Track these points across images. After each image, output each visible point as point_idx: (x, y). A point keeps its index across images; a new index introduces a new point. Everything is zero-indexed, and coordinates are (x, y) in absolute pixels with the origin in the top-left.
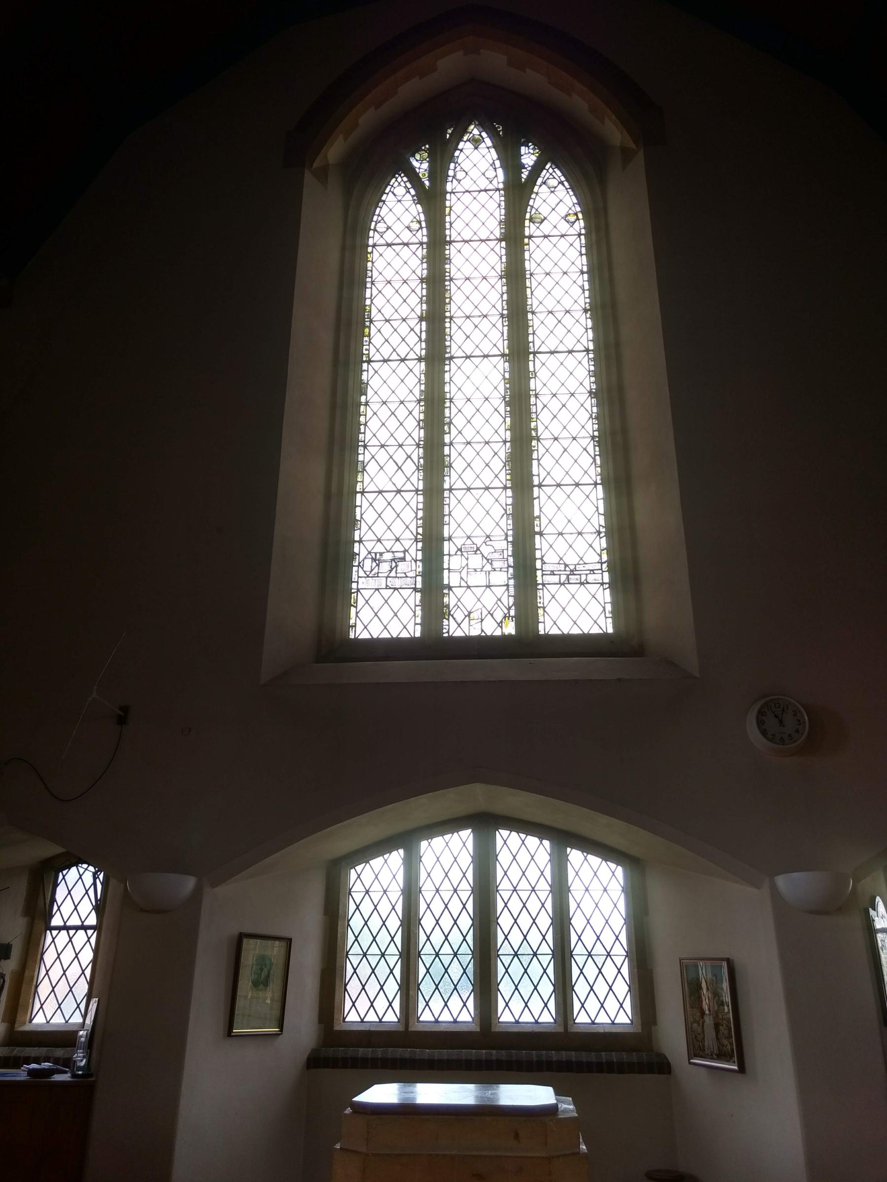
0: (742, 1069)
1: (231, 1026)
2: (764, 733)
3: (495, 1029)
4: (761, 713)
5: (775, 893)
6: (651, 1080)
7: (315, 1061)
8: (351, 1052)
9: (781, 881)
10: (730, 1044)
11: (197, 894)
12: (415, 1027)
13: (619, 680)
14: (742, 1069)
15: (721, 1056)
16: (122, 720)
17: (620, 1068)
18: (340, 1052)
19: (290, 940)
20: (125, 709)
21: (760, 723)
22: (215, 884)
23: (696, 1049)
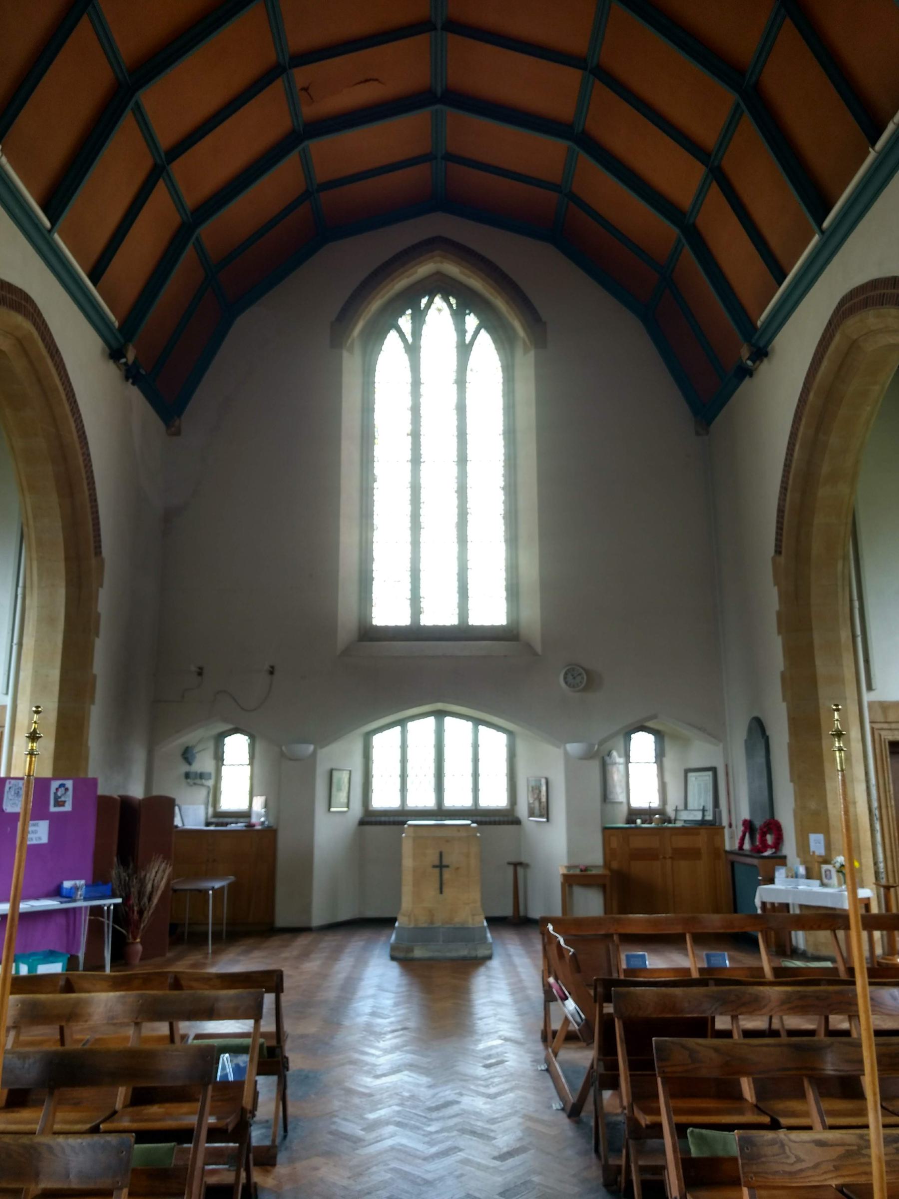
0: (548, 821)
1: (330, 806)
2: (566, 683)
3: (444, 808)
4: (566, 674)
5: (566, 753)
7: (362, 823)
8: (378, 819)
10: (544, 812)
11: (314, 753)
12: (406, 808)
13: (505, 656)
14: (548, 821)
15: (541, 816)
16: (272, 673)
17: (499, 823)
18: (373, 819)
19: (350, 771)
20: (272, 667)
21: (565, 678)
22: (322, 747)
23: (532, 814)
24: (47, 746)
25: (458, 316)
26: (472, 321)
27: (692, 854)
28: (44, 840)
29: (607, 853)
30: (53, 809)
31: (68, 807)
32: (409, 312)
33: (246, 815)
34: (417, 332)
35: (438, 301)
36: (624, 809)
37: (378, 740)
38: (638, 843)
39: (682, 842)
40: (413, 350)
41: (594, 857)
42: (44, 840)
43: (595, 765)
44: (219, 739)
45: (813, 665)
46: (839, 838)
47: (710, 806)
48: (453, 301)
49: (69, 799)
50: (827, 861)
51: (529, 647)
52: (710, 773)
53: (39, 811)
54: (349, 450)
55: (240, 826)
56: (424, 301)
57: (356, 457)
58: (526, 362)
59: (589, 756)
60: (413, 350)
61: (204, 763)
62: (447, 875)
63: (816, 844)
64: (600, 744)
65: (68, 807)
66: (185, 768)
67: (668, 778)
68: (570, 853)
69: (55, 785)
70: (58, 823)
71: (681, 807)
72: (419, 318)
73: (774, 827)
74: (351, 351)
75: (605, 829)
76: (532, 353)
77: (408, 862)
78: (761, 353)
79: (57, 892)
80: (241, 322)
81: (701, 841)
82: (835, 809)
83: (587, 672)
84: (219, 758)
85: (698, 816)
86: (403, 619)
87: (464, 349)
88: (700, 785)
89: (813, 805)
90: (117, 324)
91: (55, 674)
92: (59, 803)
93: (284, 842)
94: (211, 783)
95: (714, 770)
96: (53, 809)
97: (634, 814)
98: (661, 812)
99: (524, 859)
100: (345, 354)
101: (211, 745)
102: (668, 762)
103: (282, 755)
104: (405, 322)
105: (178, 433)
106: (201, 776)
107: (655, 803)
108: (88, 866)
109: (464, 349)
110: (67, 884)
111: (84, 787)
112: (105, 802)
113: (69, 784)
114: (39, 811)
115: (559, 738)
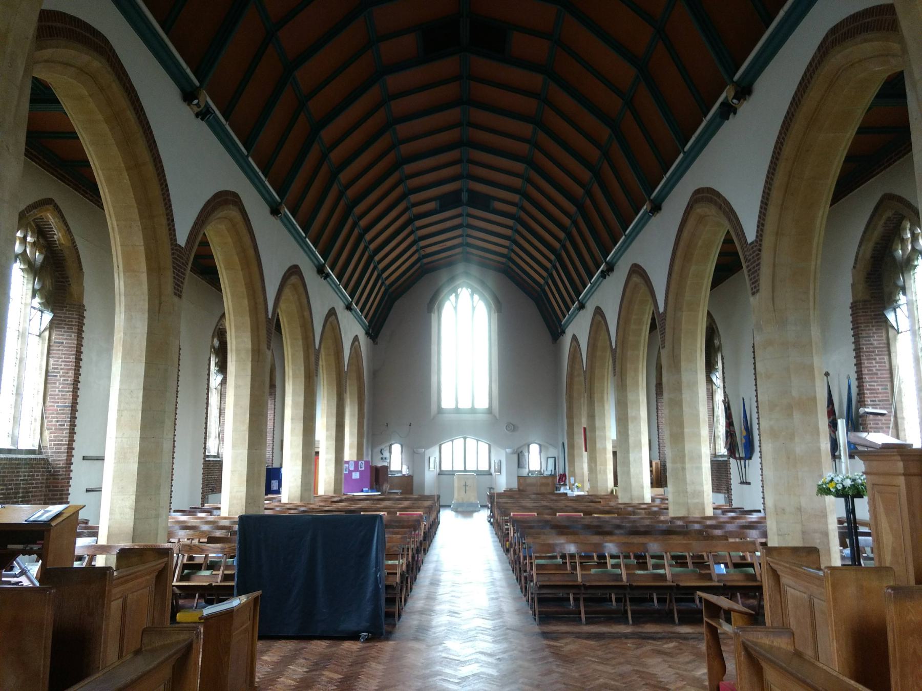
5: (506, 452)
6: (490, 476)
7: (439, 474)
9: (507, 450)
23: (495, 472)
24: (355, 451)
25: (472, 295)
26: (476, 297)
27: (547, 485)
28: (358, 477)
29: (519, 483)
30: (360, 469)
31: (363, 469)
32: (454, 294)
33: (401, 472)
34: (456, 302)
35: (464, 289)
36: (527, 470)
37: (443, 446)
38: (529, 481)
39: (544, 481)
40: (455, 308)
41: (515, 485)
42: (358, 477)
43: (515, 457)
44: (390, 446)
45: (573, 430)
46: (578, 478)
47: (553, 469)
48: (469, 290)
49: (363, 466)
50: (573, 485)
51: (495, 416)
52: (549, 459)
53: (356, 469)
54: (434, 348)
55: (399, 475)
56: (459, 290)
57: (436, 349)
58: (495, 316)
59: (513, 453)
60: (455, 308)
61: (386, 454)
62: (467, 488)
63: (572, 481)
64: (518, 448)
65: (363, 469)
66: (382, 456)
67: (542, 460)
68: (507, 484)
69: (360, 462)
70: (361, 473)
71: (545, 470)
72: (457, 296)
73: (564, 475)
74: (434, 313)
75: (518, 477)
76: (497, 314)
77: (456, 485)
78: (563, 332)
79: (362, 491)
80: (396, 303)
81: (550, 481)
82: (577, 471)
83: (514, 426)
84: (390, 452)
85: (550, 473)
86: (452, 406)
87: (474, 308)
88: (551, 461)
89: (572, 469)
90: (368, 324)
91: (356, 431)
92: (361, 468)
93: (415, 478)
94: (388, 461)
95: (555, 458)
96: (360, 469)
97: (530, 472)
98: (540, 471)
99: (493, 487)
100: (432, 314)
101: (388, 448)
102: (542, 454)
103: (414, 452)
104: (452, 297)
105: (377, 344)
106: (386, 458)
107: (538, 469)
108: (369, 484)
109: (474, 308)
110: (364, 489)
111: (367, 463)
112: (371, 467)
113: (363, 462)
114: (356, 469)
115: (504, 448)
